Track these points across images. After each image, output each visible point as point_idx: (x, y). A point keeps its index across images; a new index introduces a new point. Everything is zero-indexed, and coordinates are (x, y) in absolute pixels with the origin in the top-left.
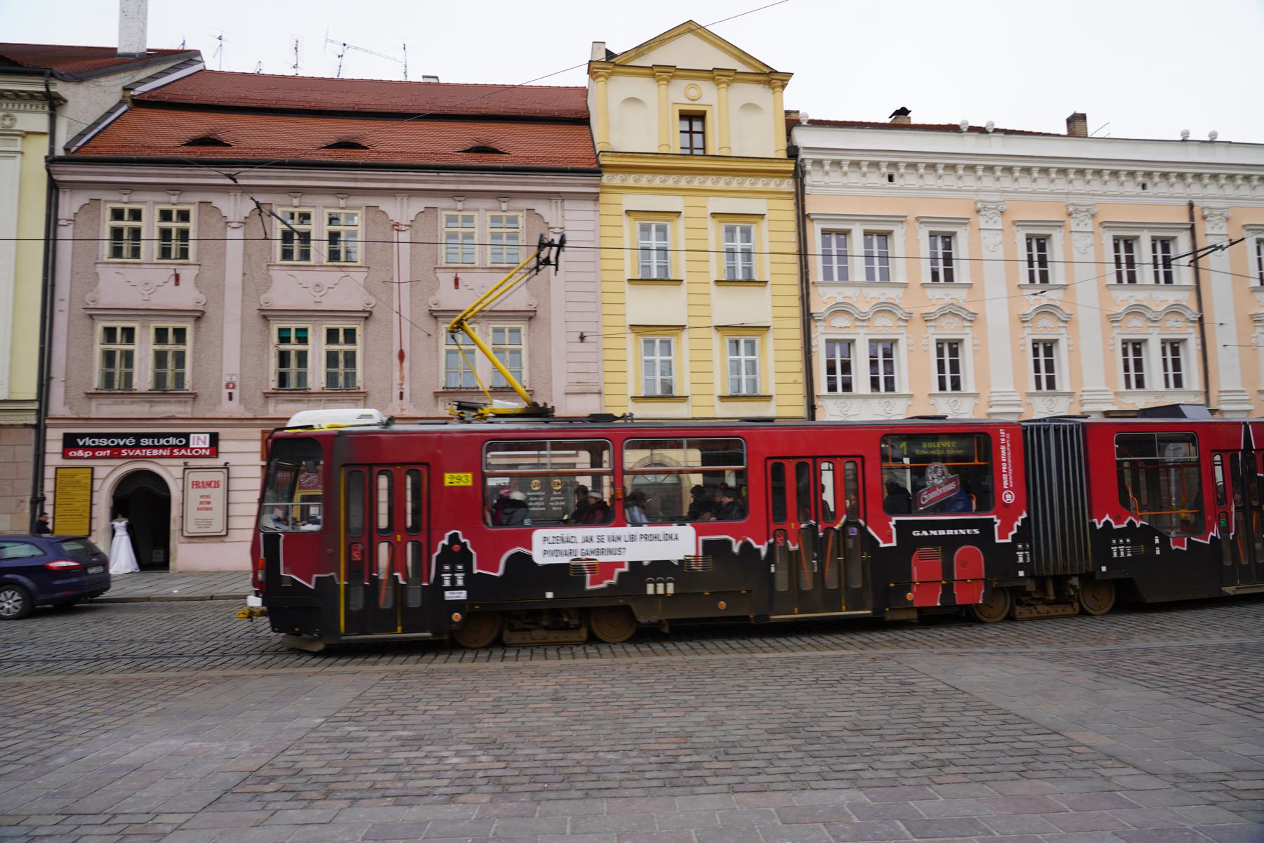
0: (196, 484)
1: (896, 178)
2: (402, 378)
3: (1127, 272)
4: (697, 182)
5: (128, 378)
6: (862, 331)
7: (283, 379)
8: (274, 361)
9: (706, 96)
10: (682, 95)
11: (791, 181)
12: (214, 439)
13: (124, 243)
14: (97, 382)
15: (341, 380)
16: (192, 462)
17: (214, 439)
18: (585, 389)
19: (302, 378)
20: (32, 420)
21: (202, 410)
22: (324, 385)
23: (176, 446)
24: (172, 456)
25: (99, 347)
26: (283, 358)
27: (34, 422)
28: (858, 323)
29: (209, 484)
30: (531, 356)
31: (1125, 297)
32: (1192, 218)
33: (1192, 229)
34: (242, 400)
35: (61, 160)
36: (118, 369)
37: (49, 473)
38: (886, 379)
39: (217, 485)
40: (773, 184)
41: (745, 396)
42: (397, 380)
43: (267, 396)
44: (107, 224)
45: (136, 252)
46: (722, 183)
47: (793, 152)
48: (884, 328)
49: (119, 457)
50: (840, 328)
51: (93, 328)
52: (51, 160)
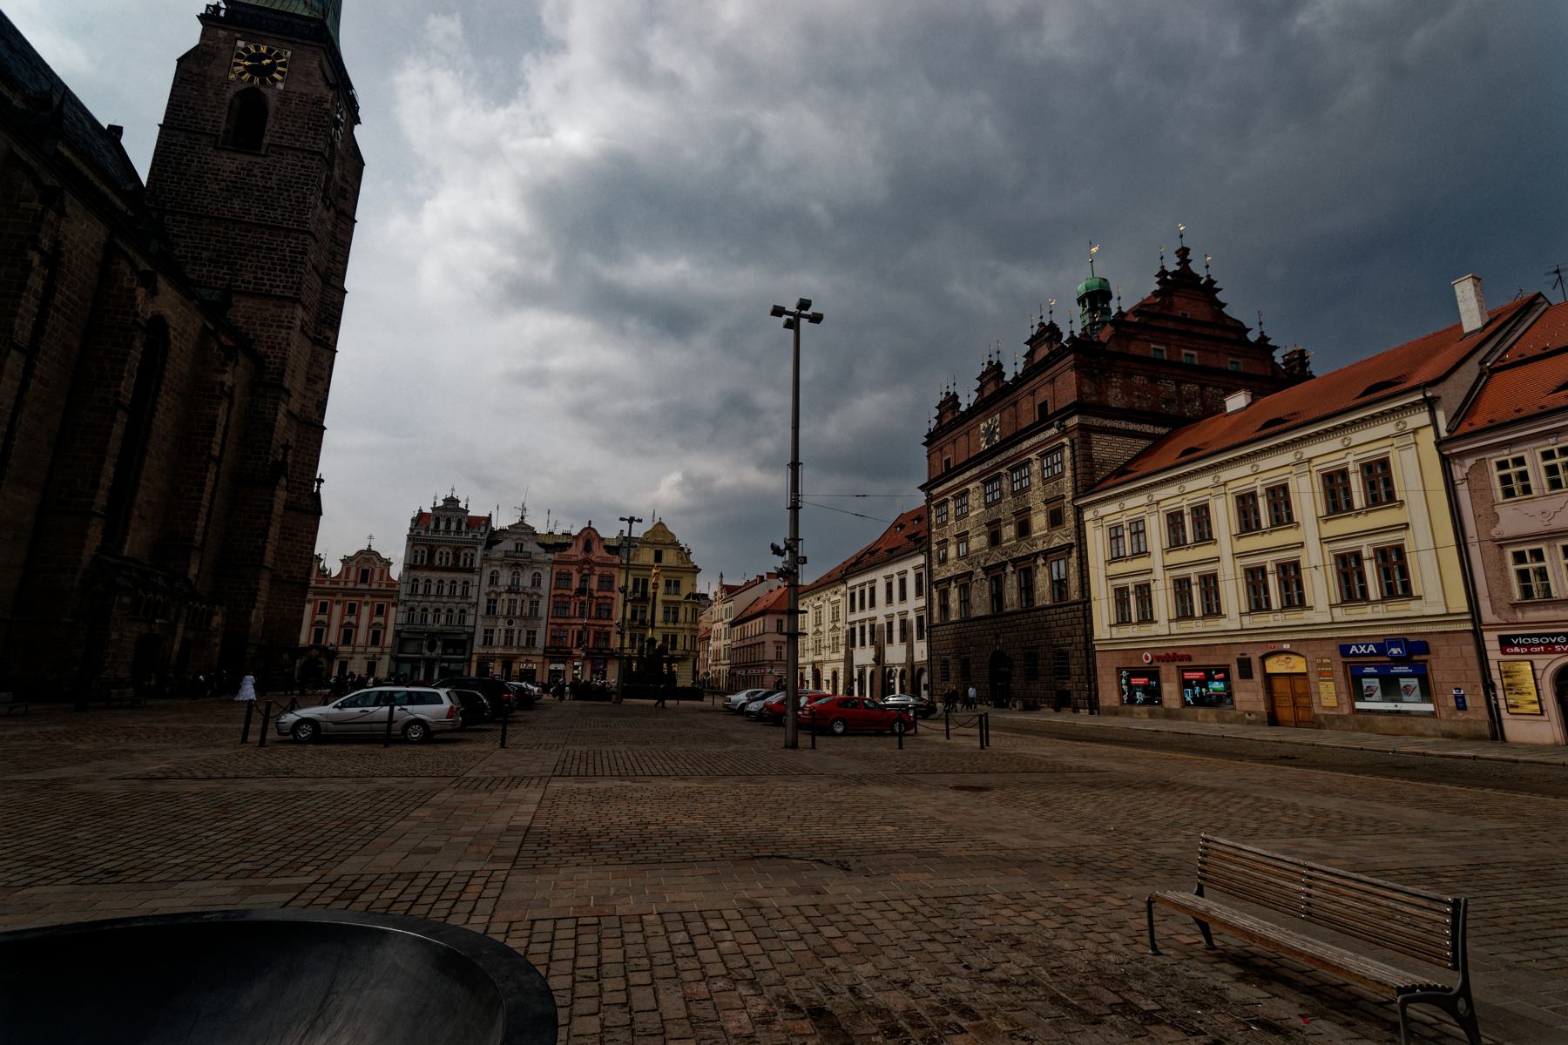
5: (1547, 589)
13: (1515, 486)
14: (1517, 595)
25: (1512, 568)
27: (1469, 626)
35: (1447, 441)
36: (1535, 583)
37: (1493, 665)
44: (1496, 475)
45: (1527, 490)
49: (1554, 652)
51: (1502, 558)
52: (1439, 443)
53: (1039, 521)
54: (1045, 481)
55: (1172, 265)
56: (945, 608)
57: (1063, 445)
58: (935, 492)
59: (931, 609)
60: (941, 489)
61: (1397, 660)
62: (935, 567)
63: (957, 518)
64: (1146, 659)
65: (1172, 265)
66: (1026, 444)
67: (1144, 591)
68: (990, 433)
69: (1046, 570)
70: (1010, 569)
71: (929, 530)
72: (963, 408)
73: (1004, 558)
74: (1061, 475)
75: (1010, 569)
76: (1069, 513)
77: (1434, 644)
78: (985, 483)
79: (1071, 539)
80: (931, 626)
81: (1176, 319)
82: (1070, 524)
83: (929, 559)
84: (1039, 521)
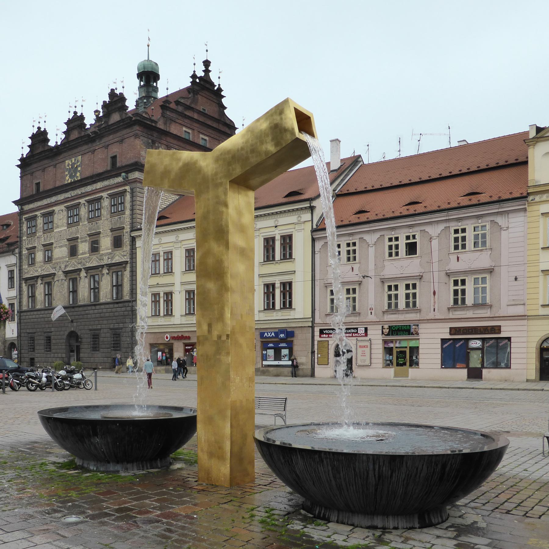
0: (361, 347)
2: (435, 302)
7: (390, 305)
8: (386, 298)
12: (366, 329)
15: (411, 305)
16: (359, 338)
17: (366, 329)
18: (517, 303)
19: (396, 305)
20: (310, 325)
21: (362, 319)
22: (404, 307)
23: (353, 333)
24: (352, 336)
26: (390, 297)
27: (310, 325)
29: (364, 347)
30: (491, 289)
34: (375, 314)
37: (316, 343)
39: (367, 347)
42: (432, 304)
43: (384, 312)
53: (106, 242)
54: (112, 214)
55: (200, 73)
56: (33, 297)
57: (125, 191)
58: (26, 207)
59: (20, 299)
60: (31, 206)
61: (282, 340)
62: (25, 267)
63: (45, 231)
64: (166, 339)
65: (200, 73)
66: (99, 185)
67: (169, 296)
68: (74, 169)
69: (109, 278)
70: (83, 274)
71: (21, 237)
72: (52, 144)
73: (79, 267)
74: (123, 211)
75: (83, 274)
76: (126, 240)
77: (297, 332)
78: (68, 208)
79: (127, 258)
80: (20, 312)
81: (199, 112)
82: (127, 248)
83: (20, 259)
84: (106, 242)
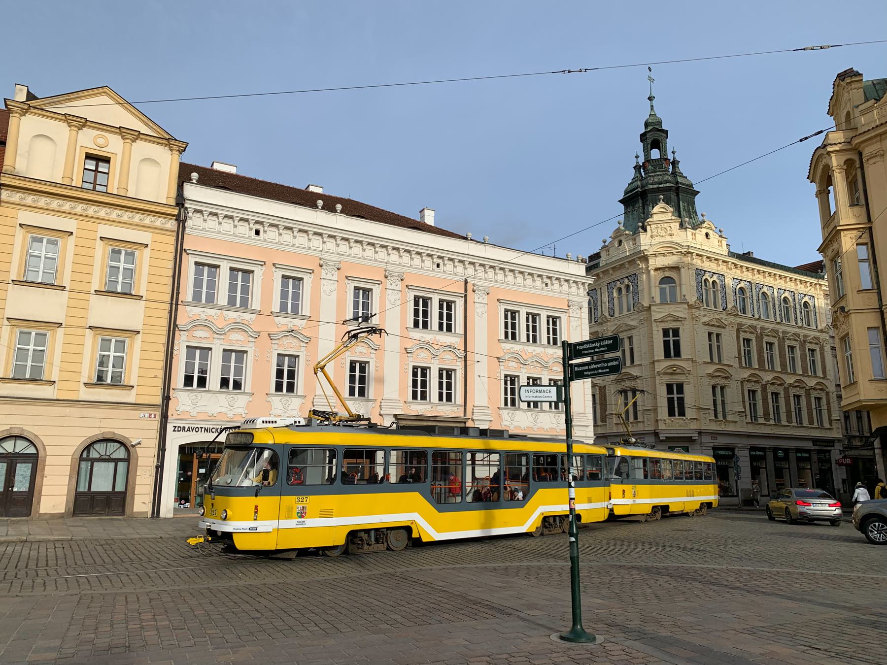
1: (261, 232)
3: (421, 321)
4: (91, 210)
6: (218, 341)
9: (113, 145)
10: (88, 140)
11: (175, 223)
28: (216, 336)
31: (419, 334)
32: (466, 290)
33: (466, 296)
38: (235, 381)
40: (159, 222)
41: (109, 385)
46: (114, 214)
47: (180, 201)
48: (237, 340)
50: (201, 338)
